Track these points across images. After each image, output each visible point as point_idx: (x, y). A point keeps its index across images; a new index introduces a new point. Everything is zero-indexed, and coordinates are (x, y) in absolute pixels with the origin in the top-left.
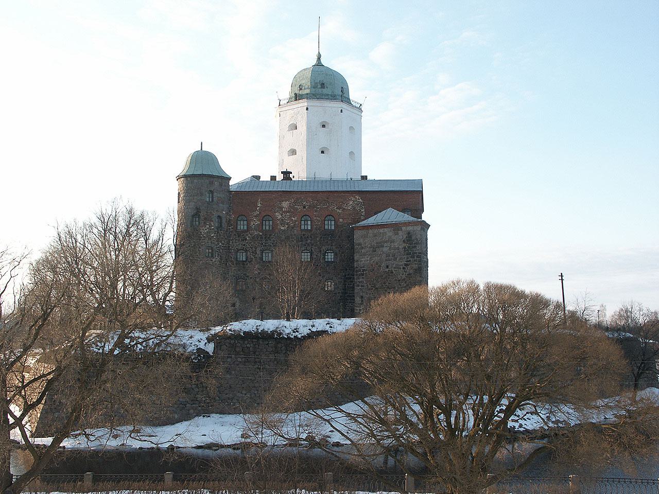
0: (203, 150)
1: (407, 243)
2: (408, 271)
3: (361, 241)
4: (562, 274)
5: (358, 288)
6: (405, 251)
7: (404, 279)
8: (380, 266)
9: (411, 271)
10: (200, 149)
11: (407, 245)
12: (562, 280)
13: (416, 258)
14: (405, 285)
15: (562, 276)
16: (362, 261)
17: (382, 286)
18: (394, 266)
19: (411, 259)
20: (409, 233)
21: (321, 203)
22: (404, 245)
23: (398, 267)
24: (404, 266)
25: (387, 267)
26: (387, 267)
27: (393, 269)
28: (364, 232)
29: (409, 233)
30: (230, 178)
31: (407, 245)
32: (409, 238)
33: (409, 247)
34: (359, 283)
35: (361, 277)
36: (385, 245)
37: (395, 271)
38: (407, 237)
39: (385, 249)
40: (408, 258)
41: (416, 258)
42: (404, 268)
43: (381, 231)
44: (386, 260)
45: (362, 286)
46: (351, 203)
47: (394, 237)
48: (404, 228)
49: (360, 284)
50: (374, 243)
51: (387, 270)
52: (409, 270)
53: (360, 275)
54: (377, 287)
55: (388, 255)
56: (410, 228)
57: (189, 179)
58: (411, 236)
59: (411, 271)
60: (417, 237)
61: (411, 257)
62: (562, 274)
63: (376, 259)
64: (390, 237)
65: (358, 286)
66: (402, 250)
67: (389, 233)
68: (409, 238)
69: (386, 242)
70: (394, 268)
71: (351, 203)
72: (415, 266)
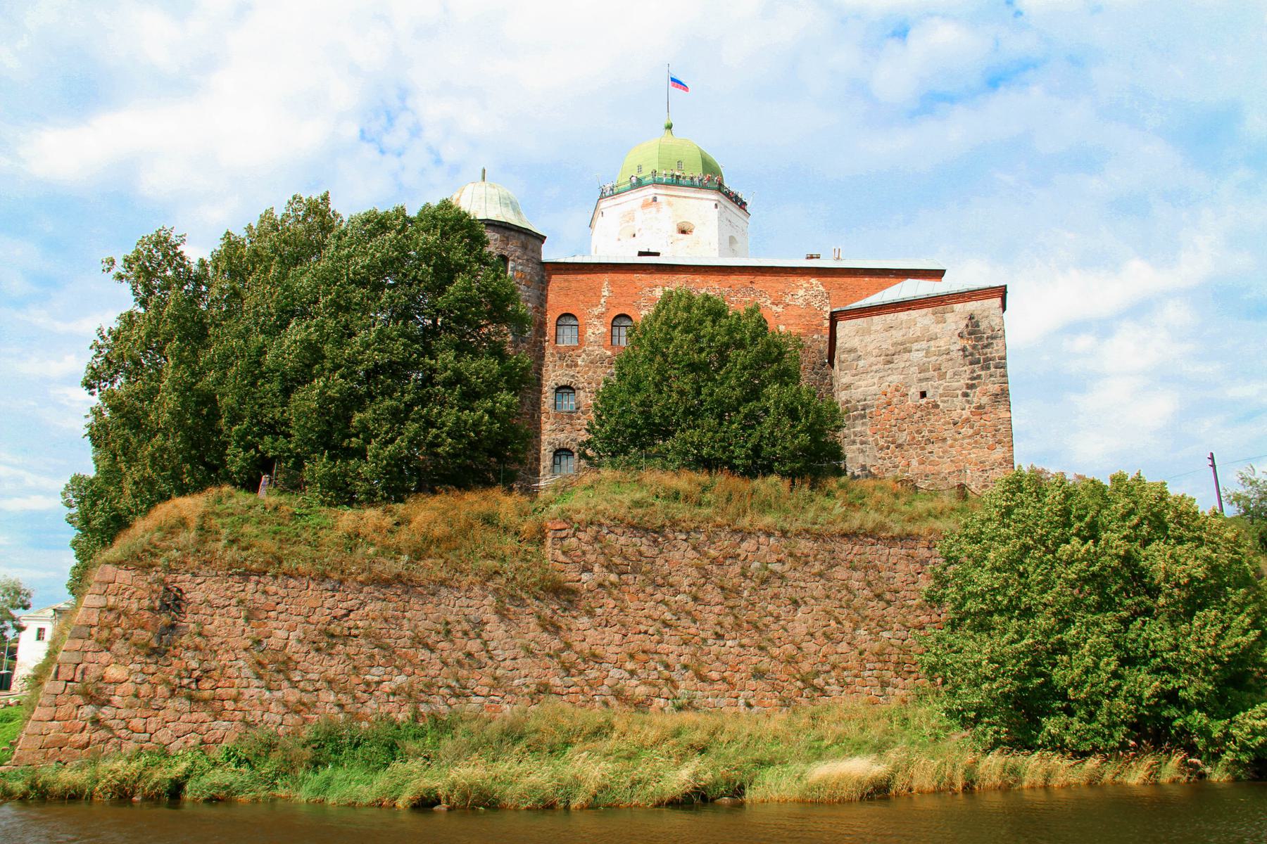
1: (968, 339)
2: (975, 399)
3: (855, 342)
4: (1212, 454)
5: (854, 447)
7: (967, 420)
9: (985, 400)
11: (968, 344)
12: (1213, 466)
13: (993, 370)
14: (971, 432)
15: (1212, 458)
16: (859, 387)
17: (914, 438)
18: (941, 391)
19: (983, 373)
21: (738, 292)
22: (961, 343)
23: (949, 394)
24: (964, 390)
25: (923, 395)
26: (923, 395)
28: (861, 322)
29: (971, 318)
30: (542, 239)
31: (968, 344)
32: (973, 327)
33: (974, 347)
34: (856, 436)
35: (859, 422)
36: (915, 347)
38: (967, 326)
39: (917, 356)
40: (973, 371)
41: (993, 370)
42: (965, 395)
43: (903, 316)
44: (920, 380)
45: (862, 443)
47: (936, 329)
48: (958, 307)
49: (858, 439)
50: (887, 345)
51: (924, 401)
52: (978, 397)
53: (856, 418)
54: (900, 442)
56: (972, 306)
58: (977, 322)
60: (993, 324)
61: (982, 368)
62: (1212, 454)
63: (895, 379)
64: (926, 328)
65: (854, 442)
66: (954, 355)
68: (973, 327)
69: (917, 340)
70: (941, 395)
71: (801, 292)
72: (994, 388)
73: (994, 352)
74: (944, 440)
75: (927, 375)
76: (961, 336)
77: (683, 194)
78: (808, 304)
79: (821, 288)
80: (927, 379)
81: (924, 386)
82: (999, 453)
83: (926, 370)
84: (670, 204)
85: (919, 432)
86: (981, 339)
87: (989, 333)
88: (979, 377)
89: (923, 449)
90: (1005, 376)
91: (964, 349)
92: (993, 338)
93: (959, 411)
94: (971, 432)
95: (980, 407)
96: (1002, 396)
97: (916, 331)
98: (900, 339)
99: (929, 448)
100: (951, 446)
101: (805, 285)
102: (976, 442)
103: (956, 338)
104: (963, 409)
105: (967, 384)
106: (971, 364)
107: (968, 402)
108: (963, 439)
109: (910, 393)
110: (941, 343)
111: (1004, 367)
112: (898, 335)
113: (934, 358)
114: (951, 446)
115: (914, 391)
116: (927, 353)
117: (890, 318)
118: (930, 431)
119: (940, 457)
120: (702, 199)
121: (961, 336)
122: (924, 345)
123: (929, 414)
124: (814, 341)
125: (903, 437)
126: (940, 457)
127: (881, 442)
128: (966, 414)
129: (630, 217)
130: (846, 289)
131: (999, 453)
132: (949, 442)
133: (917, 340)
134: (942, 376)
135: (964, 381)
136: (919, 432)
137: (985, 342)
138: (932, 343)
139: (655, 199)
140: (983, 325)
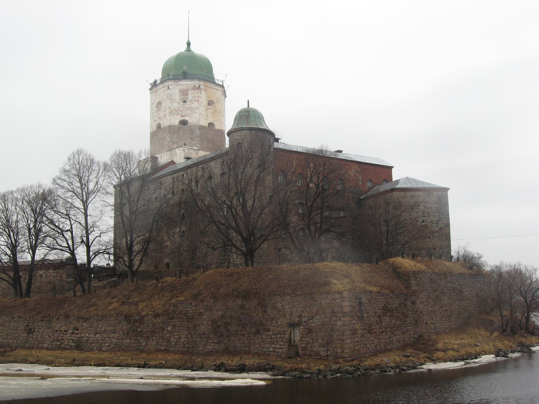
0: (250, 106)
2: (440, 225)
6: (437, 210)
10: (247, 106)
14: (438, 236)
19: (442, 217)
27: (428, 224)
37: (429, 225)
40: (439, 216)
42: (437, 223)
44: (423, 216)
46: (353, 170)
48: (435, 193)
51: (424, 224)
55: (423, 213)
57: (253, 132)
70: (429, 223)
74: (430, 238)
77: (212, 86)
80: (425, 217)
84: (205, 90)
88: (441, 218)
93: (434, 228)
100: (432, 240)
101: (354, 168)
102: (440, 239)
104: (436, 228)
105: (437, 220)
107: (438, 226)
108: (436, 238)
109: (419, 220)
114: (432, 240)
116: (425, 207)
119: (428, 243)
120: (218, 89)
123: (425, 228)
126: (428, 243)
129: (184, 93)
132: (432, 238)
139: (199, 87)
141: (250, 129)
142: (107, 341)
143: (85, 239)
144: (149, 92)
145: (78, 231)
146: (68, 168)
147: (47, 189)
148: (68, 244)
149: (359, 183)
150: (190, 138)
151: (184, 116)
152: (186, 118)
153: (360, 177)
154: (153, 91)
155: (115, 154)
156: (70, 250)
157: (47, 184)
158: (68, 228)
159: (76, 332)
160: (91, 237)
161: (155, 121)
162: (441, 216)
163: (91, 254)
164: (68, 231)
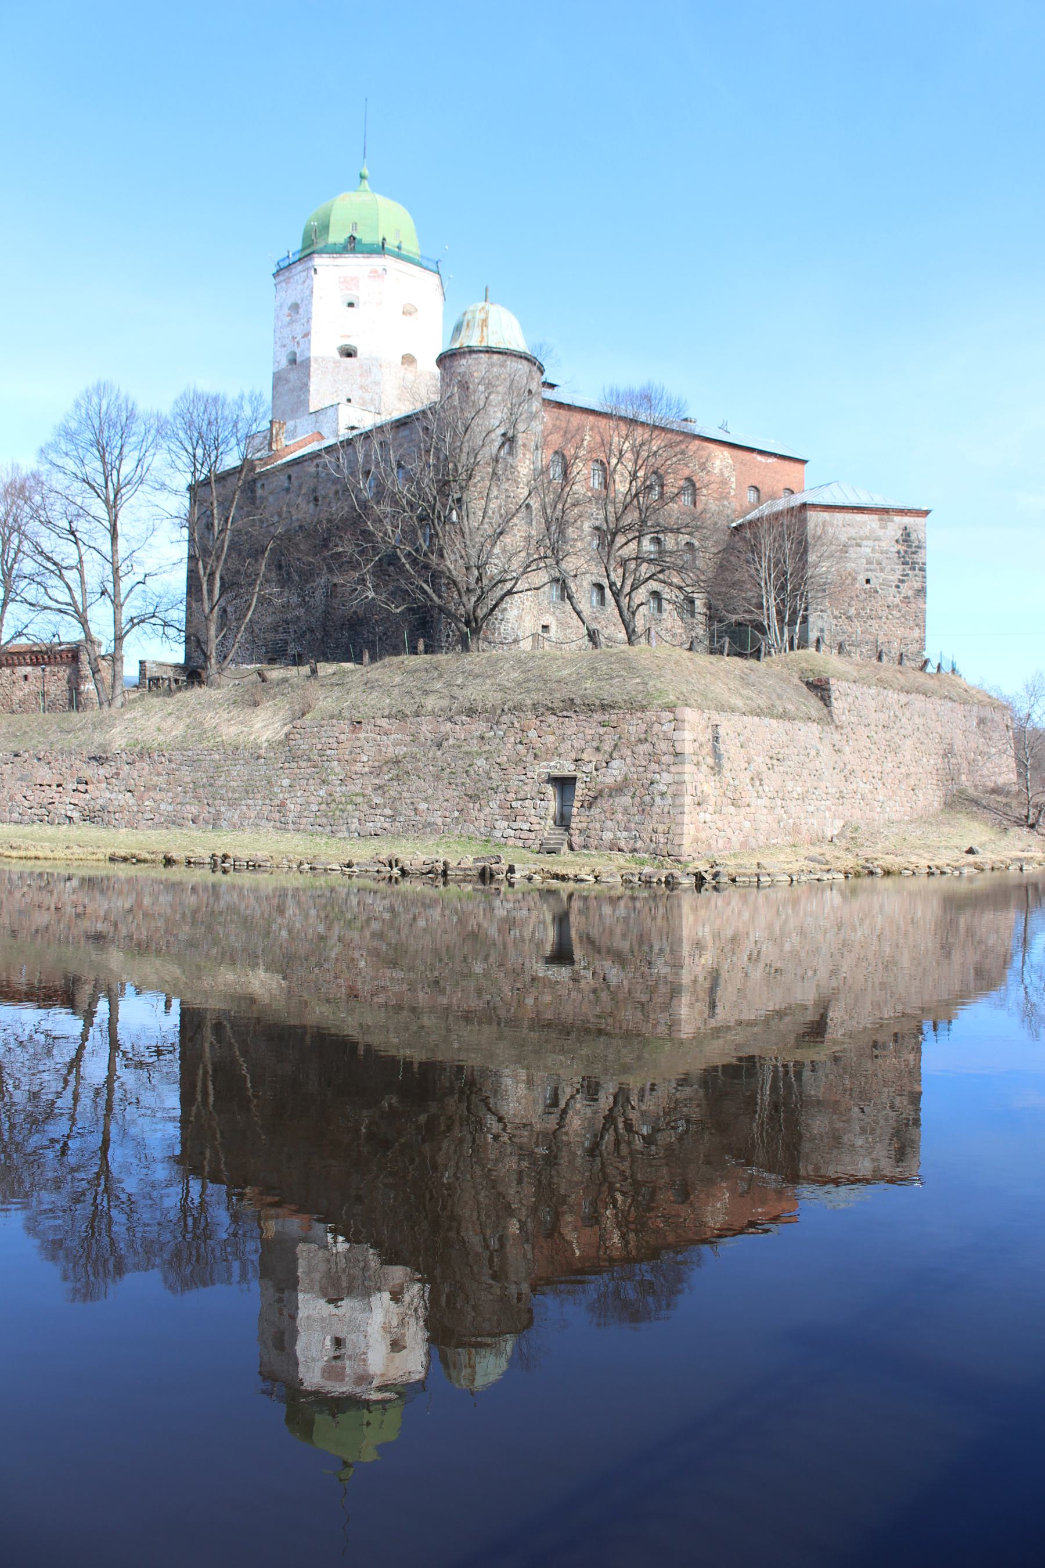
7: (897, 606)
8: (855, 579)
9: (910, 593)
13: (917, 571)
20: (906, 529)
23: (885, 584)
25: (868, 581)
26: (868, 581)
29: (906, 529)
32: (906, 537)
33: (906, 552)
36: (864, 543)
40: (904, 570)
41: (917, 571)
42: (898, 587)
43: (859, 517)
44: (867, 570)
45: (822, 611)
47: (881, 533)
51: (868, 586)
52: (906, 590)
55: (869, 563)
56: (907, 520)
59: (910, 593)
61: (910, 569)
64: (872, 530)
67: (871, 521)
68: (906, 537)
69: (867, 538)
70: (881, 584)
72: (917, 585)
73: (919, 558)
75: (872, 567)
76: (897, 541)
78: (722, 474)
79: (730, 461)
81: (870, 575)
82: (916, 633)
83: (872, 563)
85: (863, 609)
86: (910, 546)
87: (916, 543)
88: (907, 575)
89: (865, 622)
90: (925, 577)
91: (898, 552)
92: (918, 547)
94: (898, 615)
95: (906, 597)
96: (921, 592)
97: (866, 531)
98: (854, 535)
99: (870, 622)
103: (893, 543)
106: (903, 564)
107: (899, 593)
110: (883, 544)
111: (924, 570)
112: (852, 532)
113: (877, 555)
115: (862, 578)
117: (849, 516)
118: (871, 610)
121: (897, 541)
122: (870, 543)
124: (724, 506)
125: (852, 611)
127: (836, 613)
128: (897, 601)
130: (745, 465)
131: (916, 633)
132: (884, 619)
133: (867, 538)
134: (882, 570)
135: (897, 576)
136: (863, 609)
137: (914, 550)
138: (876, 543)
140: (913, 537)
141: (489, 351)
142: (148, 808)
143: (110, 587)
144: (273, 281)
145: (96, 571)
146: (73, 425)
147: (25, 471)
148: (73, 598)
149: (729, 493)
150: (361, 387)
151: (349, 337)
152: (352, 342)
153: (733, 479)
154: (281, 278)
155: (184, 397)
156: (76, 612)
157: (29, 463)
158: (73, 561)
159: (82, 787)
160: (125, 584)
161: (284, 346)
162: (908, 572)
163: (124, 618)
164: (72, 568)
